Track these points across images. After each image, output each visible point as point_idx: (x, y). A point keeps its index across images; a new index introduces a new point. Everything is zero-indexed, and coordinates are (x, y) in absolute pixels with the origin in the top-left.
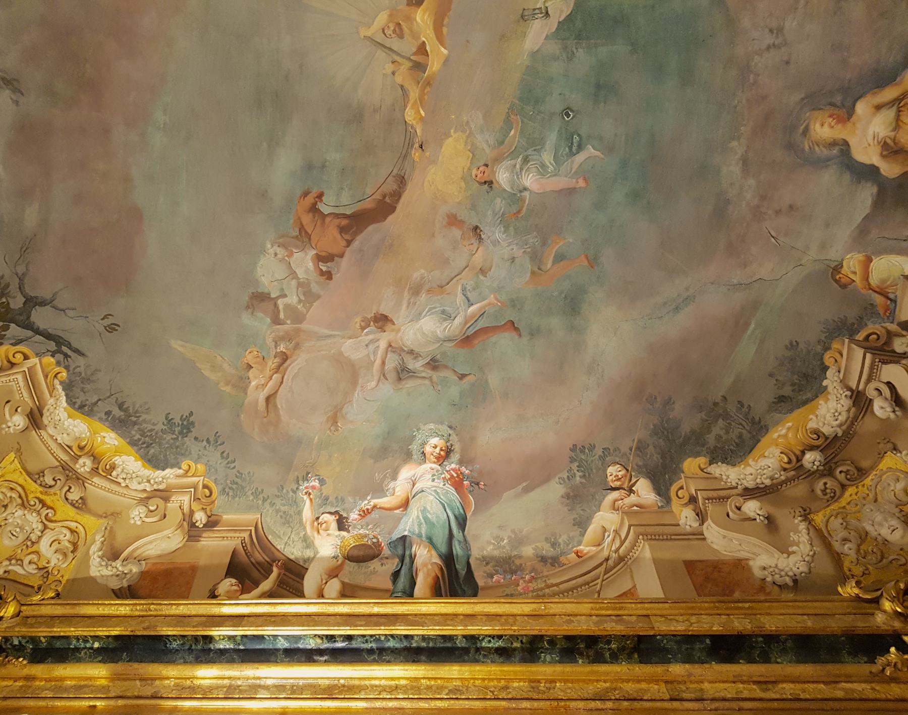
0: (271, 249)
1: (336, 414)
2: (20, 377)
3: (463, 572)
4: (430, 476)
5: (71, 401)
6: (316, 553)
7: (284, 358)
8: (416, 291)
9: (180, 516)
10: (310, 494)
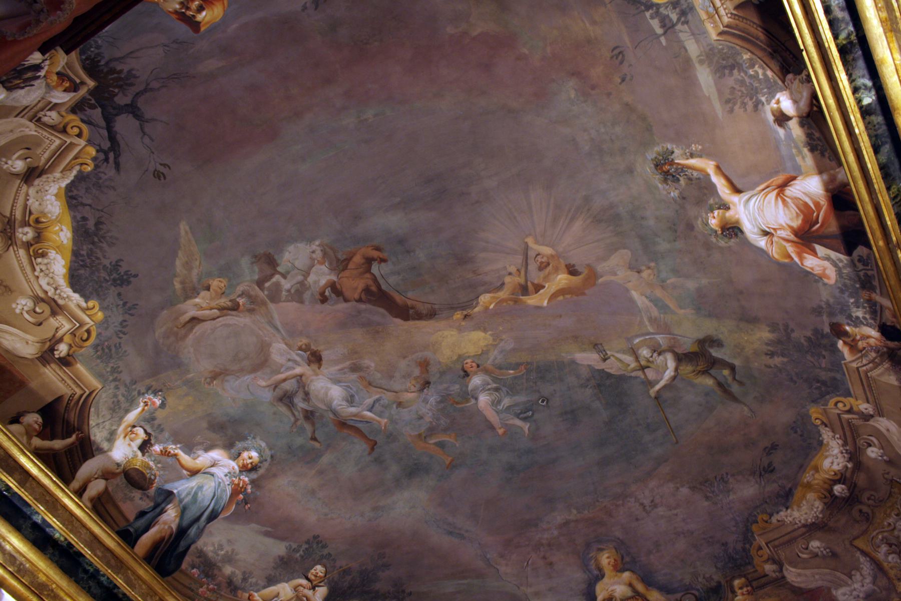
0: (315, 245)
1: (220, 374)
2: (58, 142)
3: (181, 549)
4: (226, 471)
5: (69, 188)
6: (110, 450)
7: (235, 307)
8: (355, 368)
9: (50, 335)
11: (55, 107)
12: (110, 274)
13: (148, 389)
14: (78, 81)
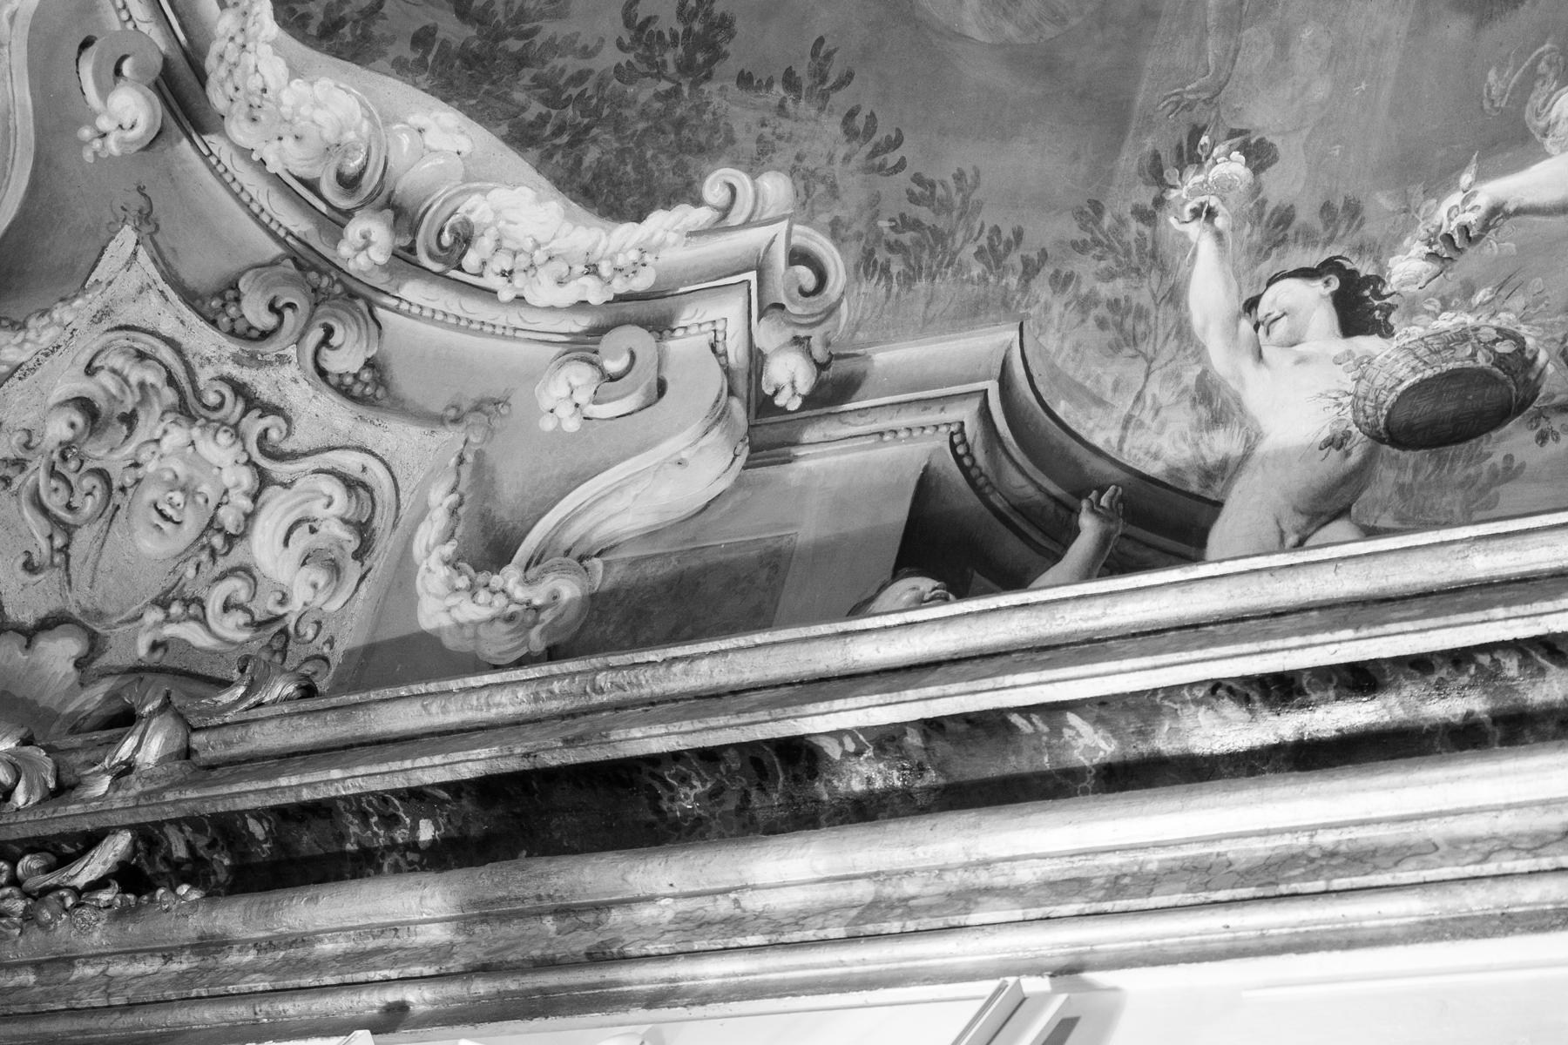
9: (715, 381)
10: (1211, 214)
12: (659, 72)
13: (1155, 173)
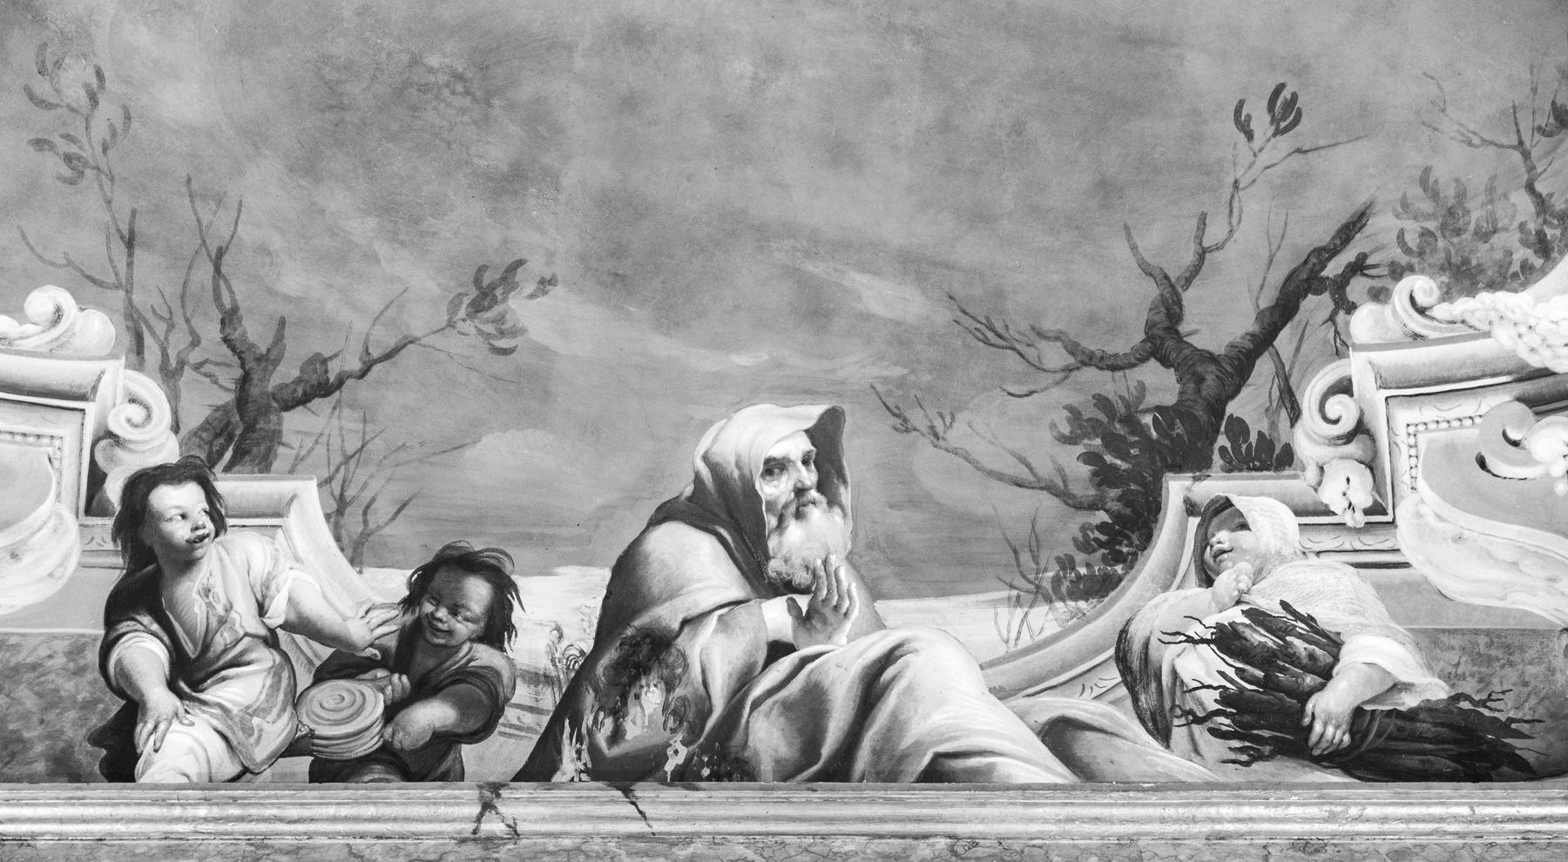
2: (1405, 416)
11: (1310, 512)
14: (1194, 522)
